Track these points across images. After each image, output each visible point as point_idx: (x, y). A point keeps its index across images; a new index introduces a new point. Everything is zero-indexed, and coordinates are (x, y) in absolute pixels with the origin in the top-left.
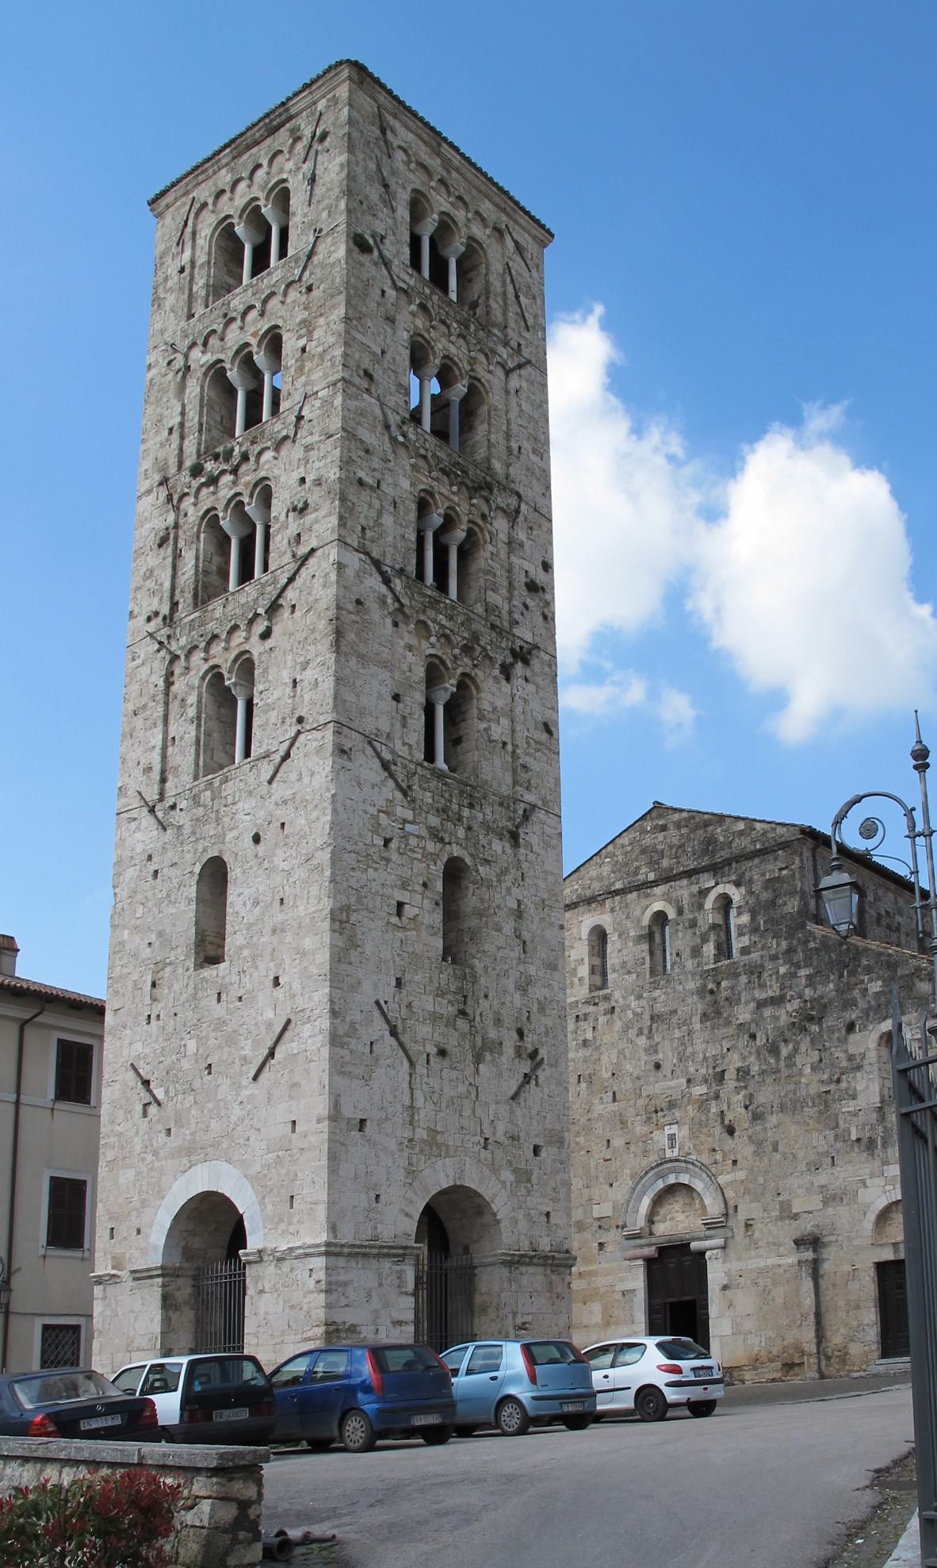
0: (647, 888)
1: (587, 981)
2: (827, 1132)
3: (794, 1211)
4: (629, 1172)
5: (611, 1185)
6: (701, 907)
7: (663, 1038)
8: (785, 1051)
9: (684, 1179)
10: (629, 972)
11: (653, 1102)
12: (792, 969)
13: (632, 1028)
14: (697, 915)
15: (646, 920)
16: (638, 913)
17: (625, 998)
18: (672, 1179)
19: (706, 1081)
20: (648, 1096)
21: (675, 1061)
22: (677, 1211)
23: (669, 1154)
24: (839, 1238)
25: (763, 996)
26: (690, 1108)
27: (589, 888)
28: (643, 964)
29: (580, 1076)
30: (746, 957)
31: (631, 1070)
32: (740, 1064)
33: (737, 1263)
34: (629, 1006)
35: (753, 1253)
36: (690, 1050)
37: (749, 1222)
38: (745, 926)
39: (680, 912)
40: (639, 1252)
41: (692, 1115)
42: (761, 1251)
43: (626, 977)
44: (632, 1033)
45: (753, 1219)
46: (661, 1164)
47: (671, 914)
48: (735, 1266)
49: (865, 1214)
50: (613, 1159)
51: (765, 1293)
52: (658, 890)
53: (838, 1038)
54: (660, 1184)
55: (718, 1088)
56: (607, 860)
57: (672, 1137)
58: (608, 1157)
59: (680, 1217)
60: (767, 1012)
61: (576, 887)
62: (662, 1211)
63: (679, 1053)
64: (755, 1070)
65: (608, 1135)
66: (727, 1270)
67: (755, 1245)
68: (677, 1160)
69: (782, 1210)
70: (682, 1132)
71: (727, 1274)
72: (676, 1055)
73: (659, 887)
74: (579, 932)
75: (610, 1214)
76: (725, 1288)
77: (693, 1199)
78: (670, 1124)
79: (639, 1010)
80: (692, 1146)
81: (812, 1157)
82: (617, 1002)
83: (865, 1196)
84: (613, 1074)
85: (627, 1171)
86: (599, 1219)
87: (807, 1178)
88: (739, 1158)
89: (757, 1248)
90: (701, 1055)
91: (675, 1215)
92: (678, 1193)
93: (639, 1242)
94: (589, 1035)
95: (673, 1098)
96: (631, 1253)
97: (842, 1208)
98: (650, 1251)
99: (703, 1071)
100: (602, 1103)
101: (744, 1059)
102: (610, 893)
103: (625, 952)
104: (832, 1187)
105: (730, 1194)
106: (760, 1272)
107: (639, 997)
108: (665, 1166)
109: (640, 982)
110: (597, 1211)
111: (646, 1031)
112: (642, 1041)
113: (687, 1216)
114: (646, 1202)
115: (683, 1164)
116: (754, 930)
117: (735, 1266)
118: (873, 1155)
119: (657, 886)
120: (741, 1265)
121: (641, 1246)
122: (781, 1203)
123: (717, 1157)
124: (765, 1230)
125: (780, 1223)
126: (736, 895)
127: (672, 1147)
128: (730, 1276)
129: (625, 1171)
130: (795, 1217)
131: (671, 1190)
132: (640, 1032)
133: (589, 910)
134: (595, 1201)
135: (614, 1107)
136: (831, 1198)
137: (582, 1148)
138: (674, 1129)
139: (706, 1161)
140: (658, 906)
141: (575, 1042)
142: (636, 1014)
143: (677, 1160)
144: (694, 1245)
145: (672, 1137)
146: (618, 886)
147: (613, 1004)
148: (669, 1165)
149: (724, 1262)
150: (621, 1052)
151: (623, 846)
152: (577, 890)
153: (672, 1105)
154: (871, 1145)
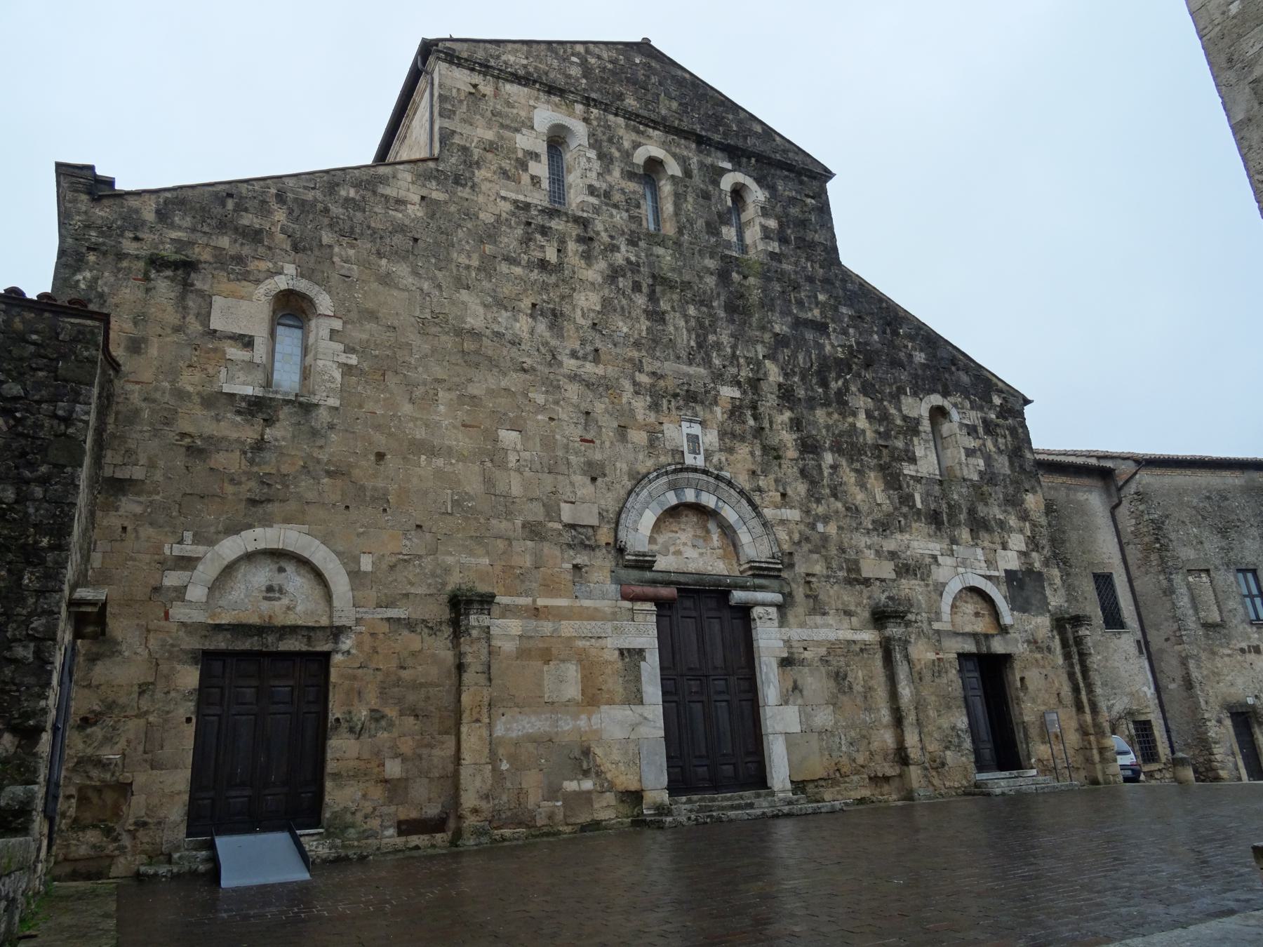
0: (640, 123)
1: (545, 184)
2: (891, 492)
3: (866, 572)
4: (625, 467)
5: (594, 480)
6: (716, 183)
7: (673, 308)
8: (835, 385)
9: (709, 500)
10: (616, 206)
11: (662, 383)
12: (832, 302)
13: (624, 276)
14: (710, 188)
15: (640, 157)
16: (627, 145)
17: (612, 237)
18: (690, 496)
19: (739, 384)
20: (654, 374)
21: (693, 343)
22: (685, 544)
23: (689, 460)
24: (919, 618)
25: (802, 315)
26: (718, 410)
27: (546, 74)
28: (638, 206)
29: (534, 305)
30: (774, 264)
31: (625, 330)
32: (781, 380)
33: (799, 630)
34: (617, 249)
35: (818, 619)
36: (711, 338)
37: (808, 579)
38: (772, 231)
39: (688, 173)
40: (649, 590)
41: (721, 419)
42: (830, 619)
43: (614, 211)
44: (621, 282)
45: (814, 575)
46: (681, 470)
47: (674, 168)
48: (796, 633)
49: (941, 595)
50: (598, 442)
51: (839, 677)
52: (656, 134)
53: (890, 393)
54: (672, 499)
55: (755, 397)
56: (574, 59)
57: (693, 439)
58: (588, 437)
59: (690, 553)
60: (809, 335)
61: (525, 62)
62: (661, 539)
63: (698, 336)
64: (801, 393)
65: (584, 406)
66: (785, 638)
67: (817, 607)
68: (705, 472)
69: (849, 570)
70: (710, 438)
71: (787, 642)
72: (693, 336)
73: (657, 132)
74: (531, 119)
75: (595, 522)
76: (786, 663)
77: (708, 531)
78: (691, 421)
79: (633, 259)
80: (723, 459)
81: (877, 515)
82: (598, 233)
83: (940, 574)
84: (595, 324)
85: (622, 466)
86: (573, 526)
87: (875, 539)
88: (790, 492)
89: (824, 614)
90: (729, 350)
91: (682, 548)
92: (684, 519)
93: (648, 575)
94: (551, 255)
95: (692, 388)
96: (638, 590)
97: (916, 582)
98: (668, 592)
99: (733, 370)
100: (577, 358)
101: (786, 375)
102: (588, 98)
103: (608, 178)
104: (903, 556)
105: (782, 535)
106: (832, 647)
107: (632, 242)
108: (685, 475)
109: (634, 227)
110: (567, 513)
111: (645, 289)
112: (641, 300)
113: (701, 554)
114: (649, 518)
115: (712, 480)
116: (783, 240)
117: (796, 633)
118: (940, 530)
119: (654, 128)
120: (804, 634)
121: (654, 582)
122: (847, 561)
123: (761, 483)
124: (832, 592)
125: (848, 587)
126: (757, 195)
127: (695, 452)
128: (791, 647)
129: (618, 465)
130: (867, 582)
131: (674, 512)
132: (637, 287)
133: (548, 102)
134: (565, 497)
135: (600, 370)
136: (906, 569)
137: (542, 409)
138: (696, 429)
139: (747, 486)
140: (657, 152)
141: (526, 257)
142: (628, 260)
143: (705, 472)
144: (738, 596)
145: (693, 439)
146: (594, 95)
147: (591, 234)
148: (691, 475)
149: (781, 627)
150: (606, 302)
151: (599, 57)
152: (525, 67)
153: (692, 397)
154: (935, 519)
